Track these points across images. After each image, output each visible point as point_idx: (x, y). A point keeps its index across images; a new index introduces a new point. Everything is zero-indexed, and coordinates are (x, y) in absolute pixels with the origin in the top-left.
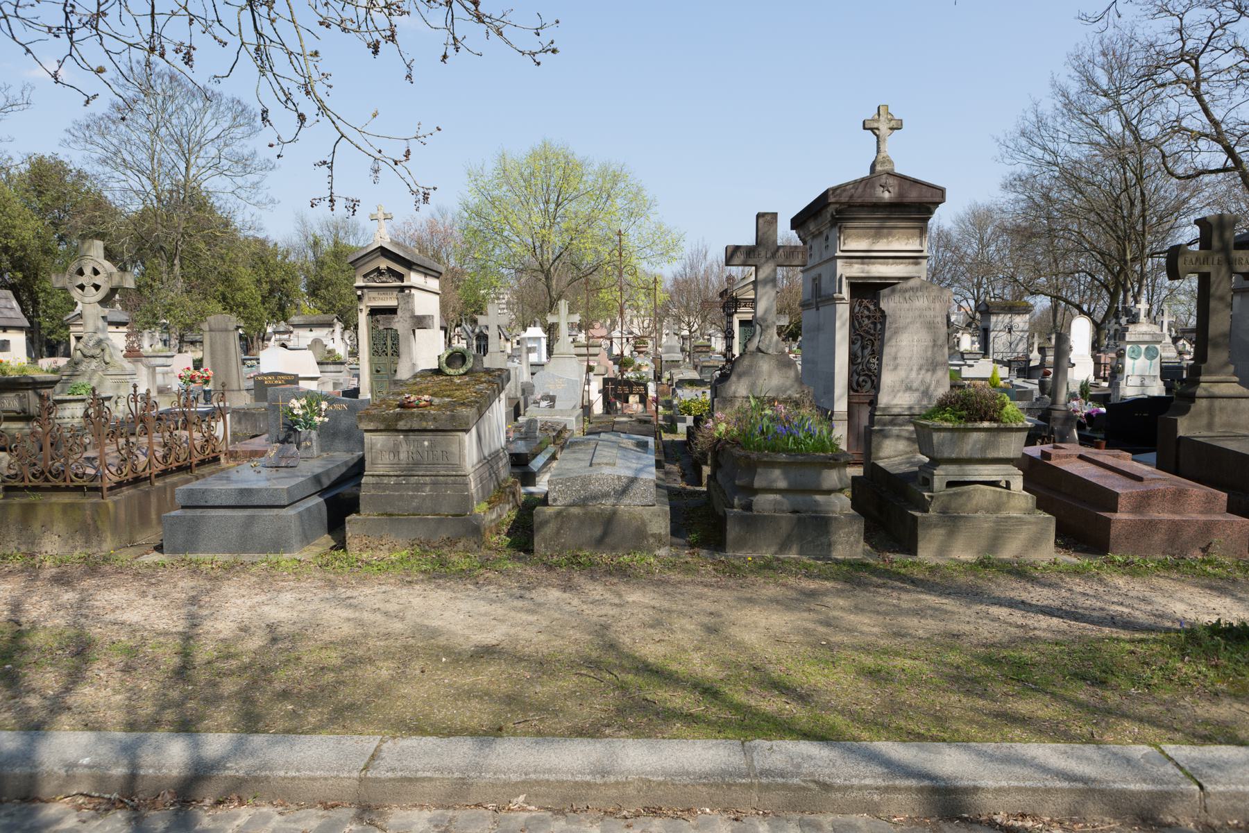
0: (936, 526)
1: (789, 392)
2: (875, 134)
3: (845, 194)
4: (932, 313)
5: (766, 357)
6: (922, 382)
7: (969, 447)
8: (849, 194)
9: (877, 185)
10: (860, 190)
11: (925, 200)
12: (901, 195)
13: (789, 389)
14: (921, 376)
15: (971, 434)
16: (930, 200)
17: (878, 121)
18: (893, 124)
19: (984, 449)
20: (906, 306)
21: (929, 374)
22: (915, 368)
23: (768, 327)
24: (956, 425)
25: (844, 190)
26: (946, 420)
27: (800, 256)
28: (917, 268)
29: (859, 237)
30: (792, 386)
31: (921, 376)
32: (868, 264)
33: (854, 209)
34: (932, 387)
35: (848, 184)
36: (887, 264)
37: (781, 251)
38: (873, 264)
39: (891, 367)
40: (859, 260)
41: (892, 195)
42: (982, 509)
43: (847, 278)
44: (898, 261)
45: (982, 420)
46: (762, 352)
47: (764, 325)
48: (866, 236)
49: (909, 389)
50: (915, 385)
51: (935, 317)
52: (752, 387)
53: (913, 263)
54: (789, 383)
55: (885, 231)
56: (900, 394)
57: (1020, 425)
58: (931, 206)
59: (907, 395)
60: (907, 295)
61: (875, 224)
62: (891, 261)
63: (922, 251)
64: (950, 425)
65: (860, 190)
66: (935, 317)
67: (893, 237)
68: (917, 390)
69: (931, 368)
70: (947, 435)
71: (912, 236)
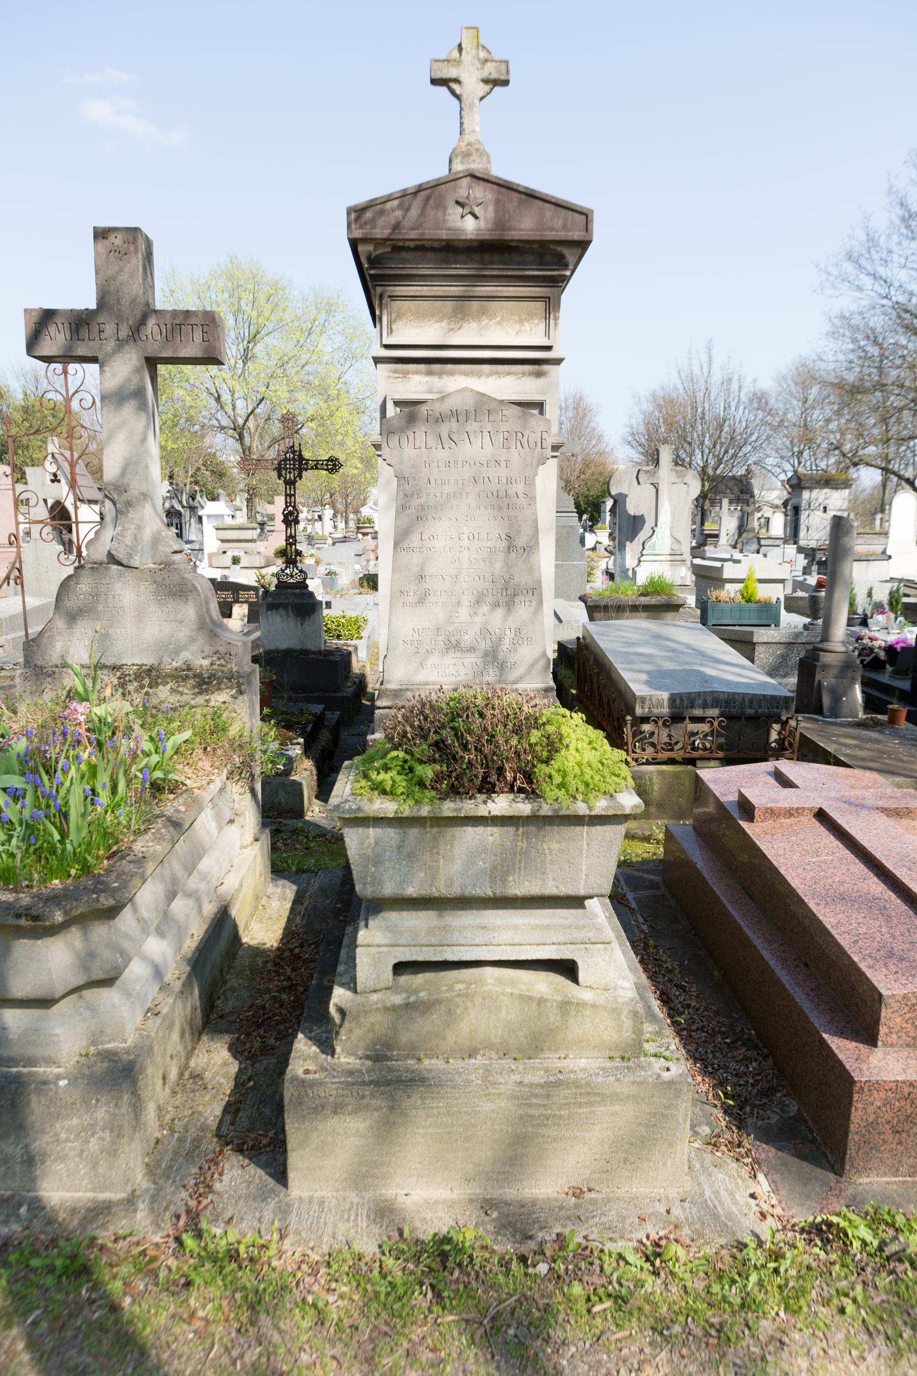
0: (337, 1109)
1: (185, 655)
2: (453, 92)
3: (381, 221)
4: (503, 472)
5: (128, 573)
6: (485, 631)
7: (456, 867)
8: (392, 221)
9: (450, 202)
10: (414, 212)
11: (551, 235)
12: (500, 224)
13: (185, 648)
14: (479, 619)
15: (458, 831)
16: (562, 235)
17: (457, 63)
18: (490, 70)
19: (499, 872)
20: (441, 455)
21: (500, 612)
22: (466, 600)
23: (129, 504)
24: (406, 810)
25: (382, 213)
26: (380, 789)
27: (198, 336)
28: (542, 381)
29: (421, 316)
30: (193, 640)
31: (479, 619)
32: (440, 374)
33: (404, 255)
34: (506, 644)
35: (388, 199)
36: (479, 375)
37: (152, 322)
38: (452, 374)
39: (412, 599)
40: (422, 367)
41: (482, 223)
42: (489, 1047)
43: (397, 403)
44: (500, 368)
45: (488, 788)
46: (120, 564)
47: (121, 500)
48: (437, 316)
49: (454, 646)
50: (467, 639)
51: (509, 481)
52: (103, 639)
53: (530, 374)
54: (183, 633)
55: (475, 305)
56: (433, 660)
57: (601, 806)
58: (566, 251)
59: (450, 660)
60: (444, 429)
61: (455, 290)
62: (486, 368)
63: (549, 348)
64: (387, 807)
65: (414, 212)
66: (509, 481)
67: (491, 318)
68: (472, 649)
69: (502, 600)
70: (391, 834)
71: (531, 315)
